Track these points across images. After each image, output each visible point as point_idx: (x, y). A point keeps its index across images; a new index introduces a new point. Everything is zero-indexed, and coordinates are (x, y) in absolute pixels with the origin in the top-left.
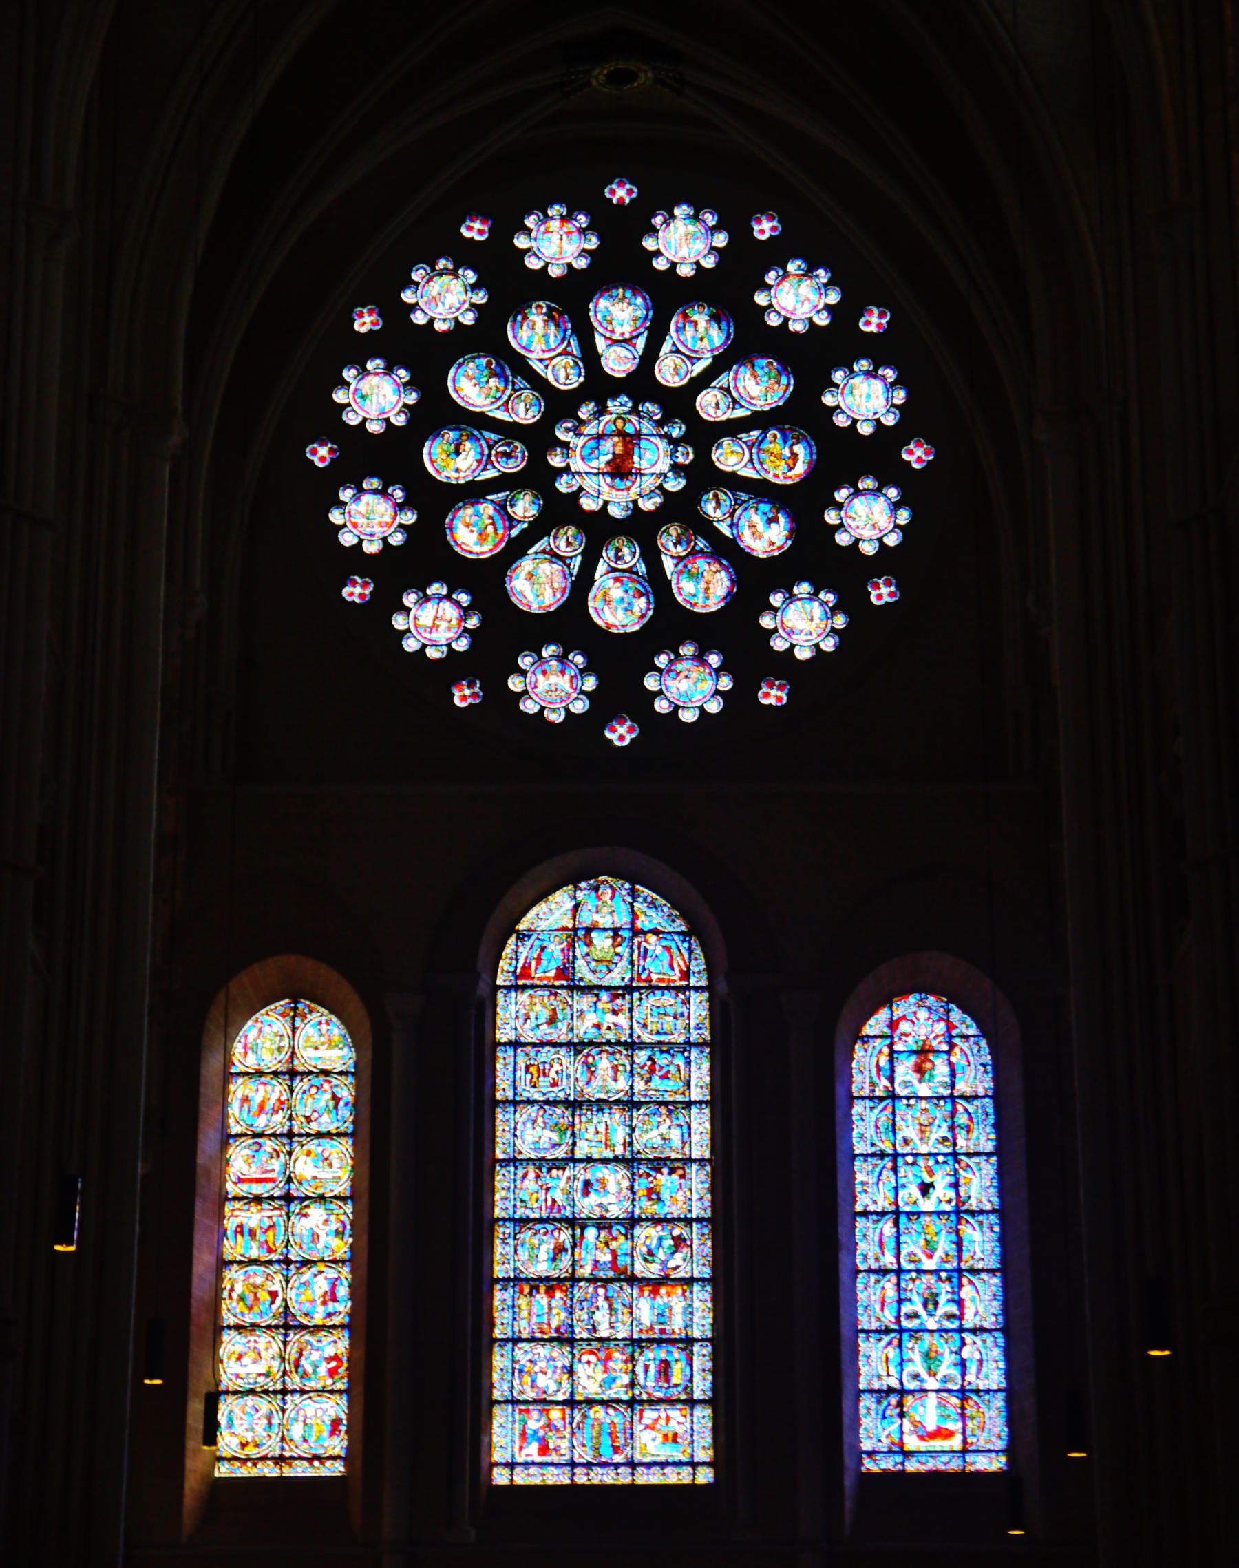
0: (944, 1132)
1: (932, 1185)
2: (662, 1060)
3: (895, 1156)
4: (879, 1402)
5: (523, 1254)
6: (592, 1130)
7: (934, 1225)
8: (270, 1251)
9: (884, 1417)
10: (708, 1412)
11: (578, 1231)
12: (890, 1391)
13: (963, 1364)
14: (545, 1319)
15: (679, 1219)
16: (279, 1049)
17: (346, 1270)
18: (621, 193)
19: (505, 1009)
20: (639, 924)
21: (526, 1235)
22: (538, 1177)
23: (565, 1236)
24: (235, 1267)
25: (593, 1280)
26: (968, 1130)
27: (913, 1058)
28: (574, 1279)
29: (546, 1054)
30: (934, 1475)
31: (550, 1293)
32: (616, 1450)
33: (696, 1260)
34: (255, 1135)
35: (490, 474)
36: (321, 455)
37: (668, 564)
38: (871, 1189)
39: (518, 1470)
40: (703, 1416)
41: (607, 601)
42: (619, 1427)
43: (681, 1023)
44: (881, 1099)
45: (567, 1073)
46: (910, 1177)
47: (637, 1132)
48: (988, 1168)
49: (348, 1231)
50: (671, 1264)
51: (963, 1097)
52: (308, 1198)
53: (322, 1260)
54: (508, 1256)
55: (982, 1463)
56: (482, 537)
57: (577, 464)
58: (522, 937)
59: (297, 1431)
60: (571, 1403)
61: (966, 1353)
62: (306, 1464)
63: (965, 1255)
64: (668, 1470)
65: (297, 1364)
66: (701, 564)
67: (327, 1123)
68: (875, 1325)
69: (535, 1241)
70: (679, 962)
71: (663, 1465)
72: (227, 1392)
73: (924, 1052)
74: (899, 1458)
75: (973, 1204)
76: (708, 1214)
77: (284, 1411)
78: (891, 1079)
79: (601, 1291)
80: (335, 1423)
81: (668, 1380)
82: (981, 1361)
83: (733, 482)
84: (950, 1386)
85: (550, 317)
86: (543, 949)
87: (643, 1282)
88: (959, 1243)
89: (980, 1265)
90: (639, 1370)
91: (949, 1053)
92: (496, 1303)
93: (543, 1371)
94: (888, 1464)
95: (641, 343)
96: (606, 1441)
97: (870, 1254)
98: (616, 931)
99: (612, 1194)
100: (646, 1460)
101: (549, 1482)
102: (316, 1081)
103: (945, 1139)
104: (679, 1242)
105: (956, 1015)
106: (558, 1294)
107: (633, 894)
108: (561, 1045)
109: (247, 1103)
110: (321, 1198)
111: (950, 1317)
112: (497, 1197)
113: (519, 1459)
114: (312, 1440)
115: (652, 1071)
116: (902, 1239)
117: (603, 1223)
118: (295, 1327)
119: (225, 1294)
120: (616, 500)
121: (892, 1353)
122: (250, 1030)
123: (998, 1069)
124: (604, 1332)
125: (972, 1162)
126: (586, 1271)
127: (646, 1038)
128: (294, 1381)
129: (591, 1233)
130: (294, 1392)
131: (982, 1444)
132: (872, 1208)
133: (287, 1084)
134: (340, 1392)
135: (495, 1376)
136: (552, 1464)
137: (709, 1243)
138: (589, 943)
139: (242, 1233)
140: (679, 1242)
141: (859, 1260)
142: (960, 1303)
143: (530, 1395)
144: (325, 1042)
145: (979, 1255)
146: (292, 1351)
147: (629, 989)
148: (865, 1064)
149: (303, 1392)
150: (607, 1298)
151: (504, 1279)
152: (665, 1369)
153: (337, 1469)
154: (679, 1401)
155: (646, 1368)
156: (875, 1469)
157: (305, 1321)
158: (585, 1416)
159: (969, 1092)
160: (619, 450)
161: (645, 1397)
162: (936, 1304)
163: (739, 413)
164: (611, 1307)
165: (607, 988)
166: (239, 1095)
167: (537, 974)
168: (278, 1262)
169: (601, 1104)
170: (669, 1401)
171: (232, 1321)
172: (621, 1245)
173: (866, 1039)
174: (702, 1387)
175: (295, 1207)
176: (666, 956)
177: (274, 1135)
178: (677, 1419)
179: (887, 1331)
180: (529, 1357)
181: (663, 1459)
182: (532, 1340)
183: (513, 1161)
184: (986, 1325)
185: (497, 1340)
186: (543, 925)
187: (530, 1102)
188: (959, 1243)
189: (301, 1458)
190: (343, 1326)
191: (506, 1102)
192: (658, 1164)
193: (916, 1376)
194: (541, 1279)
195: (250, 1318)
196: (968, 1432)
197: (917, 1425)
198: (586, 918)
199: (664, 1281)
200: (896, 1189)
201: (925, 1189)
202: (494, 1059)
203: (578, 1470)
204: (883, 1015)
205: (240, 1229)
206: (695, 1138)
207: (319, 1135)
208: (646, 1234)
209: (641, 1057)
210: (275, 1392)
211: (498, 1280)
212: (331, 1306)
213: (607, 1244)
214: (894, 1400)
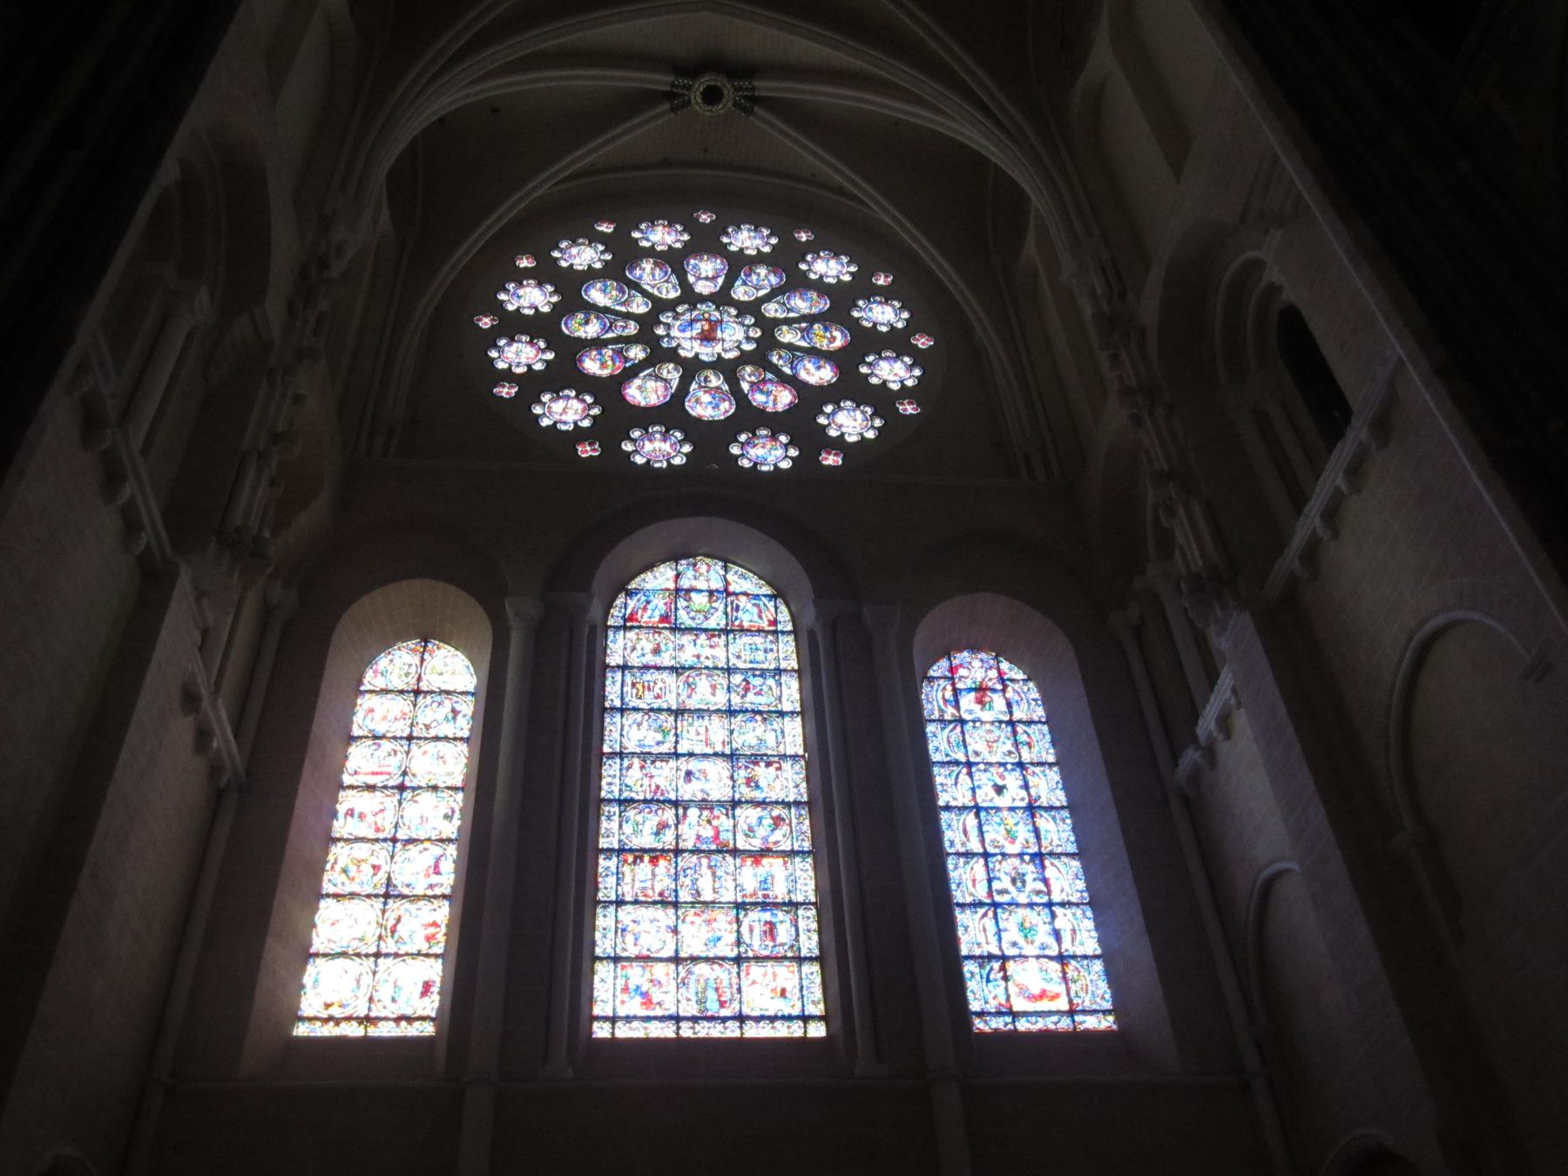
0: (1009, 746)
1: (1004, 787)
2: (756, 681)
3: (969, 765)
4: (981, 966)
5: (628, 828)
6: (692, 730)
7: (1011, 819)
8: (378, 830)
9: (988, 981)
10: (816, 968)
11: (681, 811)
12: (991, 957)
13: (1057, 935)
14: (648, 884)
15: (777, 803)
16: (407, 674)
17: (452, 850)
18: (705, 218)
19: (614, 642)
20: (731, 589)
21: (631, 813)
22: (642, 767)
23: (669, 815)
24: (340, 844)
25: (696, 851)
26: (1029, 745)
27: (973, 694)
28: (678, 852)
29: (648, 676)
30: (1045, 1034)
31: (654, 861)
32: (722, 1004)
33: (798, 832)
34: (375, 737)
35: (610, 335)
36: (486, 323)
37: (745, 386)
38: (951, 789)
39: (619, 1024)
40: (813, 971)
41: (698, 401)
42: (726, 983)
43: (770, 656)
44: (950, 722)
45: (671, 690)
46: (984, 779)
47: (736, 734)
48: (1054, 775)
49: (457, 815)
50: (771, 839)
51: (1020, 721)
52: (419, 788)
53: (429, 840)
54: (611, 830)
55: (1090, 1023)
56: (603, 365)
57: (675, 333)
58: (630, 594)
59: (384, 994)
60: (676, 960)
61: (1058, 924)
62: (392, 1024)
63: (1044, 843)
64: (778, 1024)
65: (393, 932)
66: (770, 387)
67: (447, 730)
68: (969, 900)
69: (639, 818)
70: (769, 615)
71: (773, 1019)
72: (317, 955)
73: (981, 690)
74: (1009, 1019)
75: (1044, 802)
76: (805, 798)
77: (374, 973)
78: (957, 706)
79: (704, 861)
80: (427, 987)
81: (773, 939)
82: (1074, 931)
83: (790, 347)
84: (1047, 952)
85: (656, 264)
86: (648, 602)
87: (749, 853)
88: (1036, 831)
89: (1059, 850)
90: (744, 930)
91: (1004, 691)
92: (600, 870)
93: (649, 930)
94: (998, 1023)
95: (720, 281)
96: (711, 995)
97: (957, 841)
98: (711, 593)
99: (716, 781)
100: (753, 1014)
101: (652, 1035)
102: (438, 698)
103: (1010, 753)
104: (778, 821)
105: (1005, 665)
106: (662, 863)
107: (726, 569)
108: (665, 668)
109: (375, 712)
110: (435, 788)
111: (1038, 893)
112: (604, 783)
113: (622, 1012)
114: (401, 1001)
115: (747, 689)
116: (985, 828)
117: (705, 804)
118: (396, 896)
119: (328, 866)
120: (707, 353)
121: (989, 922)
122: (383, 662)
123: (1046, 701)
124: (707, 896)
125: (1038, 770)
126: (689, 845)
127: (740, 665)
128: (389, 946)
129: (693, 813)
130: (387, 955)
131: (1087, 1005)
132: (953, 803)
133: (409, 729)
134: (436, 956)
135: (598, 935)
136: (656, 1018)
137: (807, 822)
138: (689, 600)
139: (352, 815)
140: (778, 821)
141: (947, 844)
142: (1046, 881)
143: (633, 951)
144: (453, 669)
145: (1056, 842)
146: (391, 918)
147: (726, 631)
148: (934, 698)
149: (396, 955)
150: (710, 867)
151: (609, 850)
152: (770, 930)
153: (428, 1029)
154: (785, 958)
155: (751, 930)
156: (987, 1029)
157: (406, 891)
158: (689, 972)
159: (1025, 718)
160: (706, 327)
161: (750, 954)
162: (1024, 882)
163: (792, 315)
164: (714, 874)
165: (706, 630)
166: (365, 707)
167: (645, 619)
168: (385, 840)
169: (700, 713)
170: (777, 959)
171: (332, 890)
172: (724, 823)
173: (931, 679)
174: (810, 944)
175: (408, 794)
176: (755, 610)
177: (395, 738)
178: (786, 975)
179: (981, 904)
180: (633, 917)
181: (771, 1013)
182: (636, 902)
183: (621, 755)
184: (1074, 900)
185: (600, 902)
186: (648, 586)
187: (636, 709)
188: (1036, 831)
189: (386, 1019)
190: (444, 896)
191: (613, 709)
192: (755, 759)
193: (1014, 944)
194: (644, 851)
195: (347, 889)
196: (1073, 994)
197: (1022, 990)
198: (685, 583)
199: (765, 852)
200: (973, 789)
201: (999, 790)
202: (604, 677)
203: (684, 1025)
204: (944, 663)
205: (350, 813)
206: (788, 739)
207: (437, 739)
208: (747, 815)
209: (737, 679)
210: (367, 956)
211: (603, 851)
212: (434, 879)
213: (709, 822)
214: (996, 965)
